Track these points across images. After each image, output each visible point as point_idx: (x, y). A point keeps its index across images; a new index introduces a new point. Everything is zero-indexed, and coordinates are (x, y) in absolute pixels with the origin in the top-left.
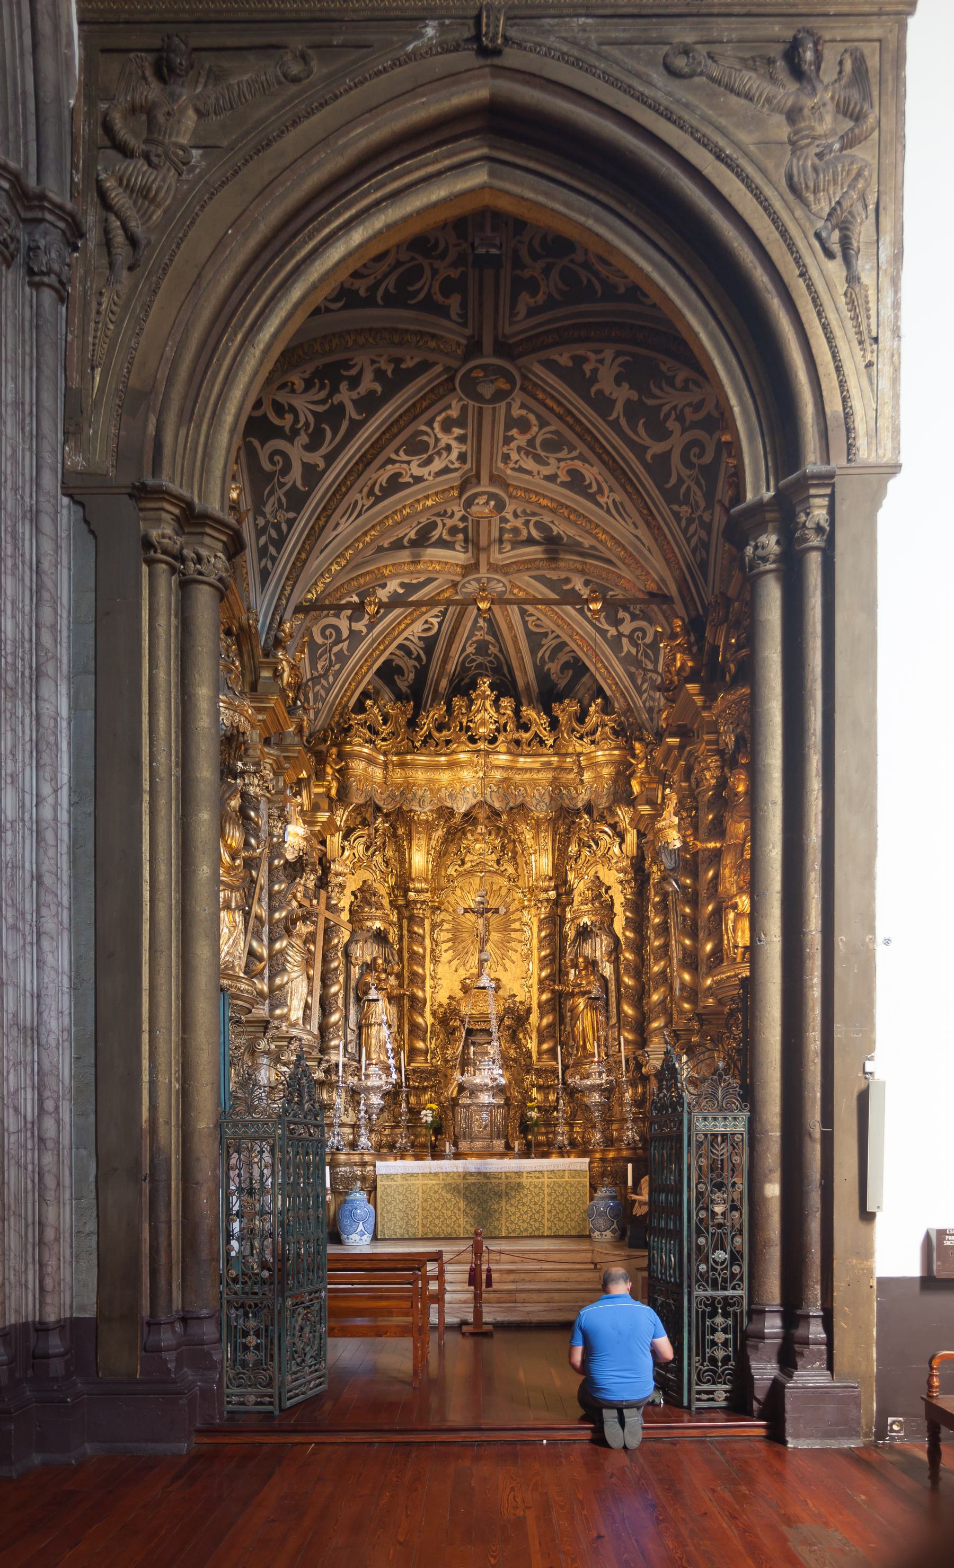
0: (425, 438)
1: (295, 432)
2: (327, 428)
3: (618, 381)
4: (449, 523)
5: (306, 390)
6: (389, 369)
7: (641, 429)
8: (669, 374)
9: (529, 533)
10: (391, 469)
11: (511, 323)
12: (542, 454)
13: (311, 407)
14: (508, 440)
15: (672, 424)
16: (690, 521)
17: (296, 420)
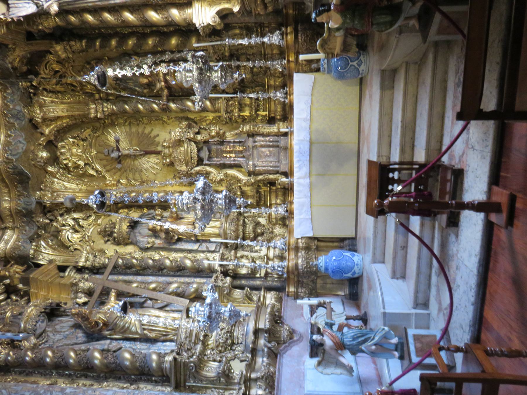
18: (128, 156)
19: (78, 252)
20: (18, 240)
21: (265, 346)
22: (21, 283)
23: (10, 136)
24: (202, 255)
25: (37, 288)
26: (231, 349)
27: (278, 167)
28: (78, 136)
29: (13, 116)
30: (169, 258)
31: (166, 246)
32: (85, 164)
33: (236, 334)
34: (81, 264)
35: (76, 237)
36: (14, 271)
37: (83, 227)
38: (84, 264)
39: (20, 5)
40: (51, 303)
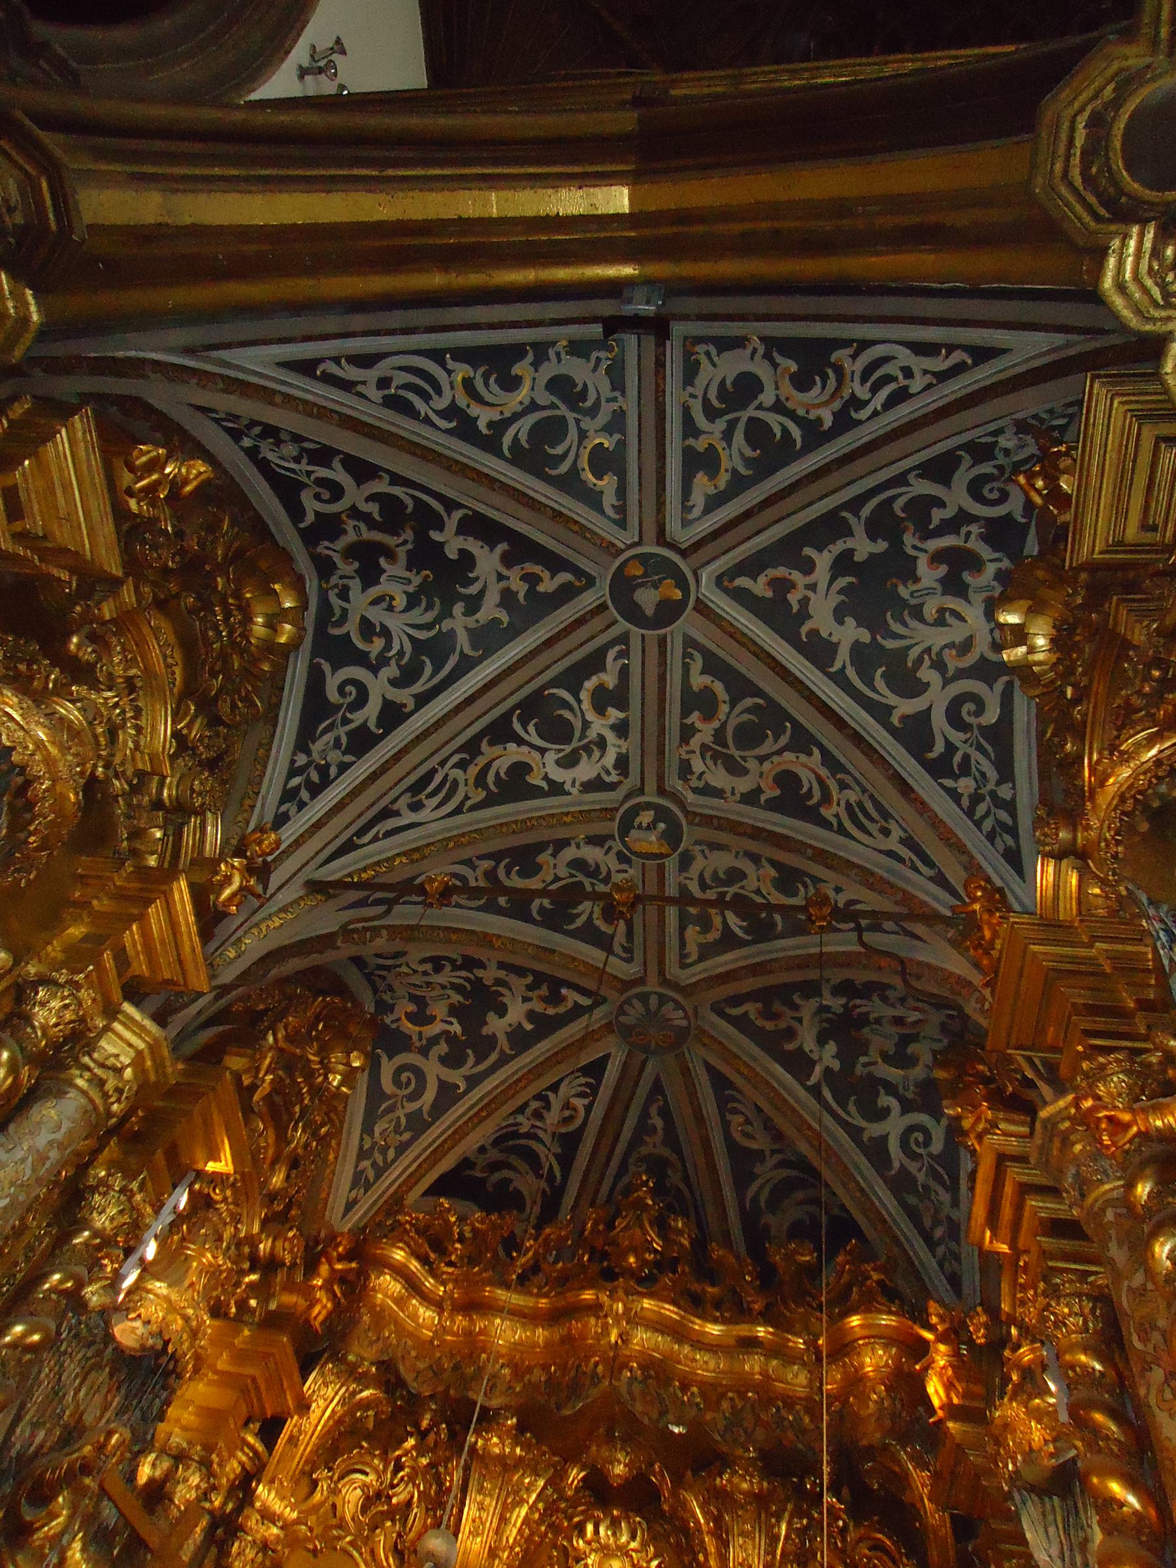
0: (567, 714)
1: (383, 661)
2: (428, 661)
3: (839, 615)
5: (408, 609)
6: (520, 588)
7: (880, 683)
8: (913, 602)
10: (513, 753)
11: (685, 523)
12: (737, 754)
13: (411, 631)
14: (687, 733)
15: (926, 674)
16: (976, 799)
17: (388, 646)
23: (684, 1388)
35: (352, 1496)
36: (319, 1301)
38: (258, 1504)
39: (1052, 1530)
40: (179, 1376)
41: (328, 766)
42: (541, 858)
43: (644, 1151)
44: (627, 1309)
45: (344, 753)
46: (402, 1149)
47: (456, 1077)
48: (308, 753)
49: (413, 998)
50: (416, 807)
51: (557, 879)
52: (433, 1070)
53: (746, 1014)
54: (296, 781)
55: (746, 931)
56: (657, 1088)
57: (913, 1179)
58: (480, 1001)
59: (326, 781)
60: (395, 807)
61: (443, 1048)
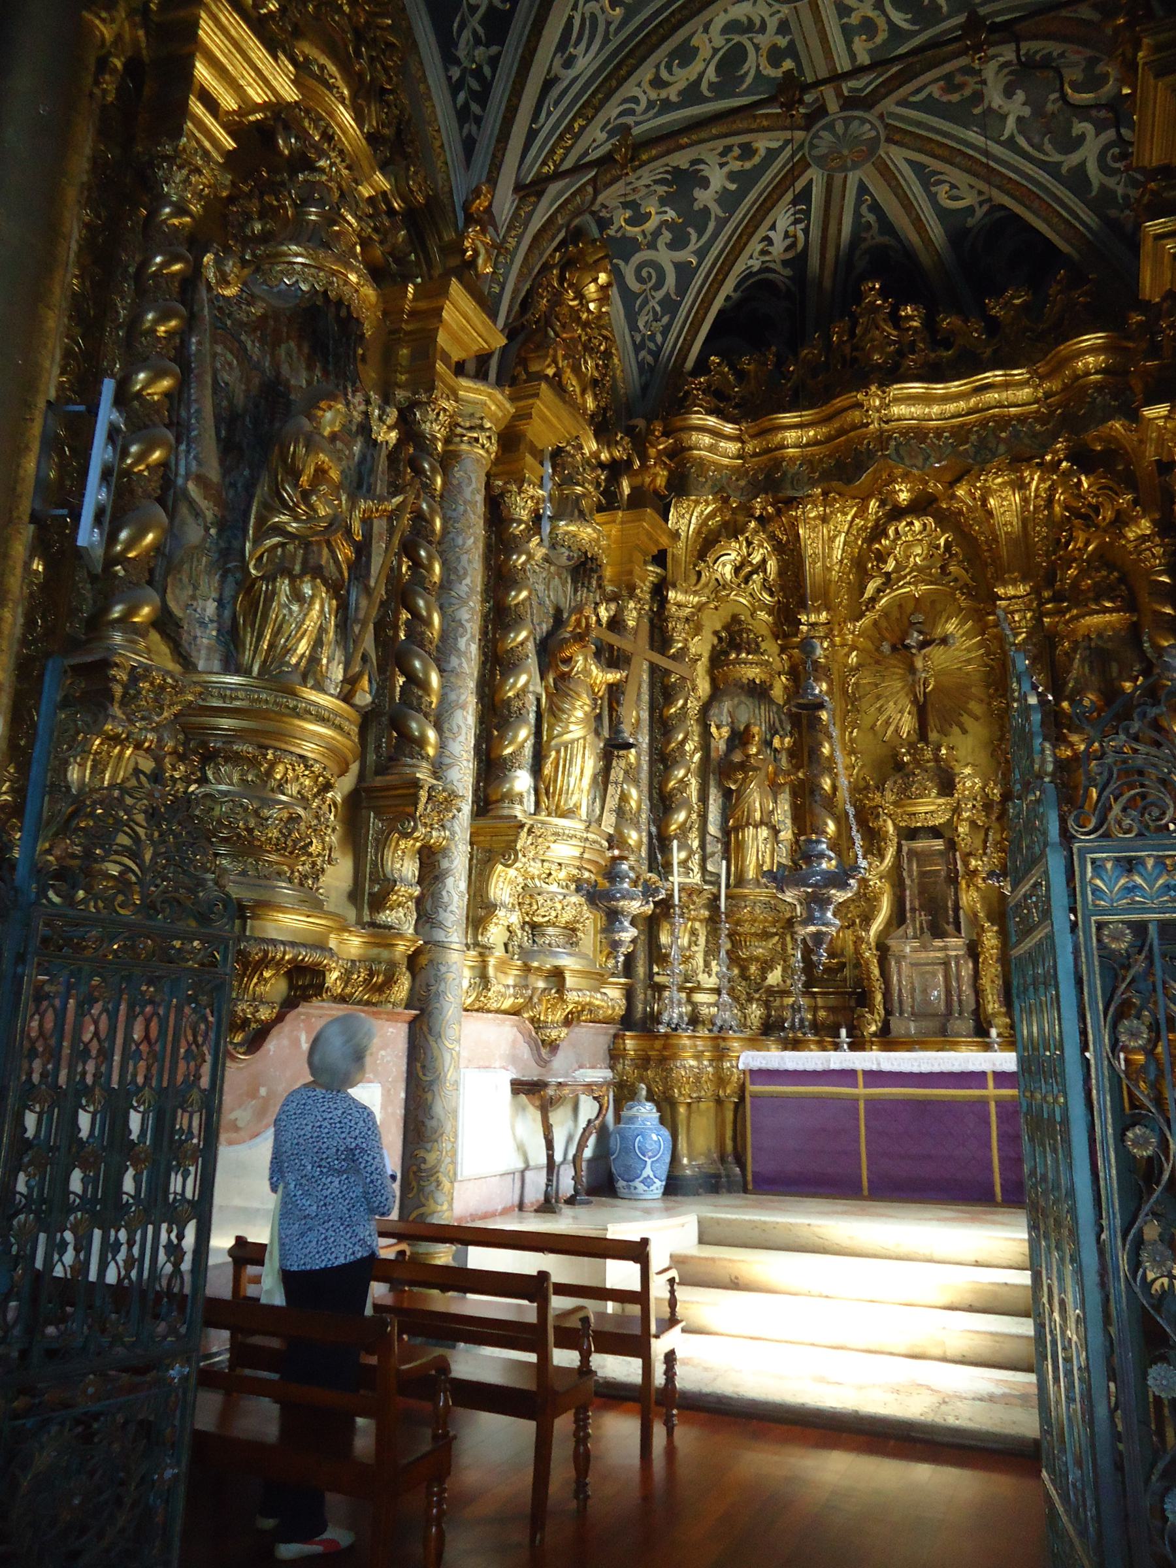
4: (764, 40)
9: (889, 21)
18: (912, 670)
19: (694, 579)
20: (719, 467)
21: (534, 989)
22: (633, 488)
24: (695, 844)
25: (622, 523)
26: (525, 923)
27: (901, 1014)
28: (951, 555)
29: (982, 440)
30: (685, 777)
31: (714, 764)
32: (888, 574)
33: (551, 930)
34: (671, 594)
37: (746, 582)
41: (480, 67)
42: (694, 42)
43: (864, 246)
44: (882, 399)
45: (487, 46)
46: (666, 331)
47: (687, 255)
48: (457, 62)
49: (625, 205)
50: (569, 63)
51: (716, 50)
52: (665, 257)
53: (930, 95)
54: (462, 96)
55: (912, 22)
56: (863, 189)
57: (1114, 192)
58: (685, 182)
59: (487, 85)
60: (552, 74)
61: (667, 236)
